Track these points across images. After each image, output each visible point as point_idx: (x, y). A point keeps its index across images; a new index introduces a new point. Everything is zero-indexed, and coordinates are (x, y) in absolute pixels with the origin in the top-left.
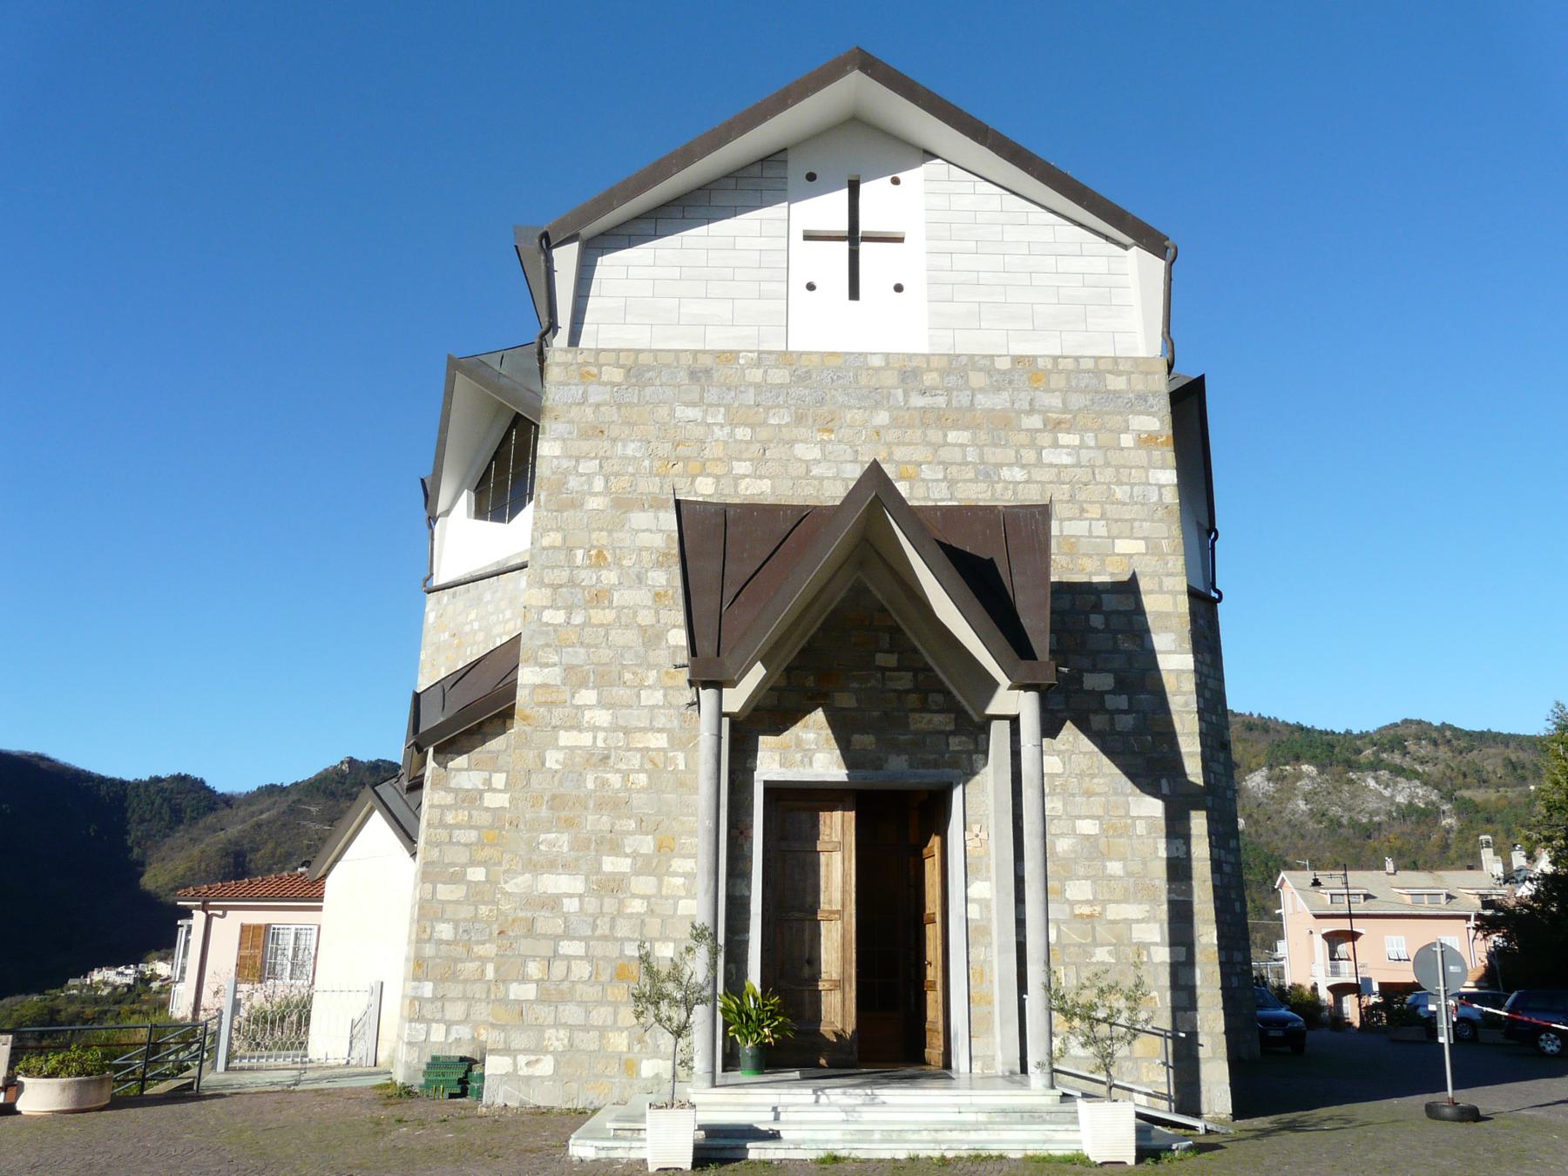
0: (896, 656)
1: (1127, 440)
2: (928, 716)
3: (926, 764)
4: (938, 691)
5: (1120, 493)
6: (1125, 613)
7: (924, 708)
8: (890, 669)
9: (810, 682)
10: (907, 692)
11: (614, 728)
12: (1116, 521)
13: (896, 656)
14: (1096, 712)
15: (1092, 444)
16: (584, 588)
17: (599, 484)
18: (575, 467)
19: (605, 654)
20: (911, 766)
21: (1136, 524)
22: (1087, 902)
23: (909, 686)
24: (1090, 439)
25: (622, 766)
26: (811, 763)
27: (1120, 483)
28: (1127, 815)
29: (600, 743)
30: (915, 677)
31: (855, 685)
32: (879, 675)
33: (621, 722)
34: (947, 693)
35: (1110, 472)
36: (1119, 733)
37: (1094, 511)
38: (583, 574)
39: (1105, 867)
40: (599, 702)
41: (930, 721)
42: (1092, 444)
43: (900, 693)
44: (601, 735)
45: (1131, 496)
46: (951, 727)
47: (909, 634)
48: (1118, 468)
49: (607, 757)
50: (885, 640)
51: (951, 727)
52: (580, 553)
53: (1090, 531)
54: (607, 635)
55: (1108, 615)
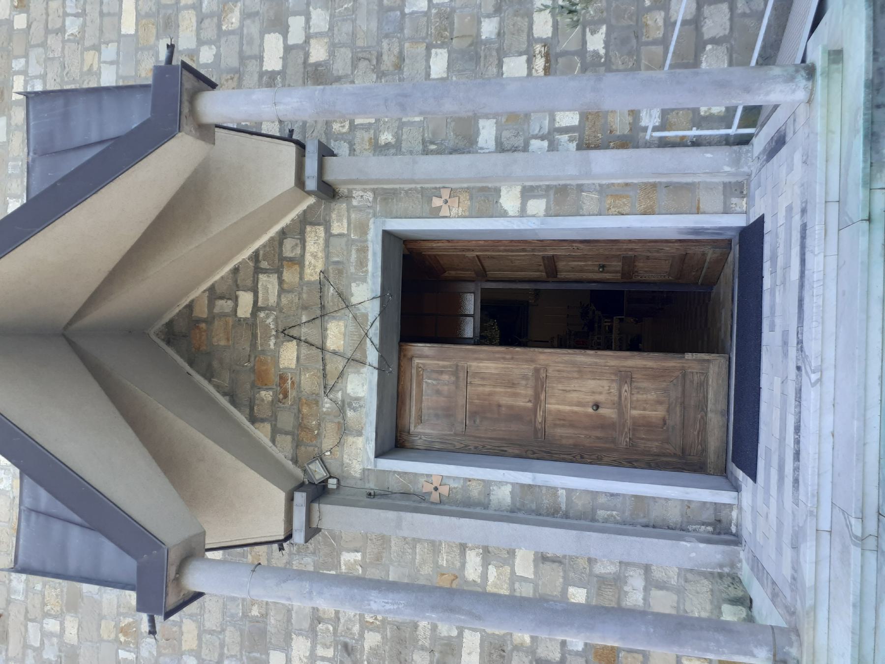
0: (241, 294)
1: (20, 21)
2: (308, 258)
3: (362, 263)
4: (281, 244)
5: (72, 26)
6: (200, 21)
7: (299, 262)
8: (256, 302)
9: (266, 395)
10: (281, 282)
11: (312, 633)
12: (101, 31)
13: (241, 294)
14: (307, 55)
15: (23, 61)
16: (160, 654)
17: (52, 625)
18: (35, 649)
19: (231, 636)
20: (364, 280)
21: (105, 10)
22: (530, 62)
23: (274, 278)
24: (18, 64)
25: (356, 629)
26: (358, 399)
27: (62, 30)
28: (426, 14)
29: (330, 653)
30: (265, 271)
31: (272, 342)
32: (262, 315)
33: (306, 625)
34: (283, 234)
35: (52, 40)
36: (331, 29)
37: (90, 57)
38: (144, 653)
39: (488, 41)
40: (282, 649)
41: (315, 256)
42: (23, 61)
43: (282, 291)
44: (320, 651)
45: (77, 15)
46: (321, 230)
47: (217, 277)
48: (47, 31)
49: (346, 646)
50: (223, 305)
51: (321, 230)
52: (122, 654)
53: (111, 63)
54: (211, 632)
55: (201, 42)
